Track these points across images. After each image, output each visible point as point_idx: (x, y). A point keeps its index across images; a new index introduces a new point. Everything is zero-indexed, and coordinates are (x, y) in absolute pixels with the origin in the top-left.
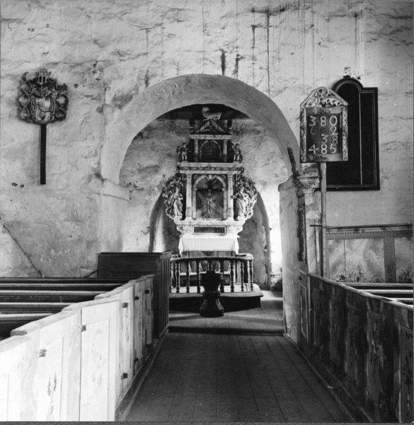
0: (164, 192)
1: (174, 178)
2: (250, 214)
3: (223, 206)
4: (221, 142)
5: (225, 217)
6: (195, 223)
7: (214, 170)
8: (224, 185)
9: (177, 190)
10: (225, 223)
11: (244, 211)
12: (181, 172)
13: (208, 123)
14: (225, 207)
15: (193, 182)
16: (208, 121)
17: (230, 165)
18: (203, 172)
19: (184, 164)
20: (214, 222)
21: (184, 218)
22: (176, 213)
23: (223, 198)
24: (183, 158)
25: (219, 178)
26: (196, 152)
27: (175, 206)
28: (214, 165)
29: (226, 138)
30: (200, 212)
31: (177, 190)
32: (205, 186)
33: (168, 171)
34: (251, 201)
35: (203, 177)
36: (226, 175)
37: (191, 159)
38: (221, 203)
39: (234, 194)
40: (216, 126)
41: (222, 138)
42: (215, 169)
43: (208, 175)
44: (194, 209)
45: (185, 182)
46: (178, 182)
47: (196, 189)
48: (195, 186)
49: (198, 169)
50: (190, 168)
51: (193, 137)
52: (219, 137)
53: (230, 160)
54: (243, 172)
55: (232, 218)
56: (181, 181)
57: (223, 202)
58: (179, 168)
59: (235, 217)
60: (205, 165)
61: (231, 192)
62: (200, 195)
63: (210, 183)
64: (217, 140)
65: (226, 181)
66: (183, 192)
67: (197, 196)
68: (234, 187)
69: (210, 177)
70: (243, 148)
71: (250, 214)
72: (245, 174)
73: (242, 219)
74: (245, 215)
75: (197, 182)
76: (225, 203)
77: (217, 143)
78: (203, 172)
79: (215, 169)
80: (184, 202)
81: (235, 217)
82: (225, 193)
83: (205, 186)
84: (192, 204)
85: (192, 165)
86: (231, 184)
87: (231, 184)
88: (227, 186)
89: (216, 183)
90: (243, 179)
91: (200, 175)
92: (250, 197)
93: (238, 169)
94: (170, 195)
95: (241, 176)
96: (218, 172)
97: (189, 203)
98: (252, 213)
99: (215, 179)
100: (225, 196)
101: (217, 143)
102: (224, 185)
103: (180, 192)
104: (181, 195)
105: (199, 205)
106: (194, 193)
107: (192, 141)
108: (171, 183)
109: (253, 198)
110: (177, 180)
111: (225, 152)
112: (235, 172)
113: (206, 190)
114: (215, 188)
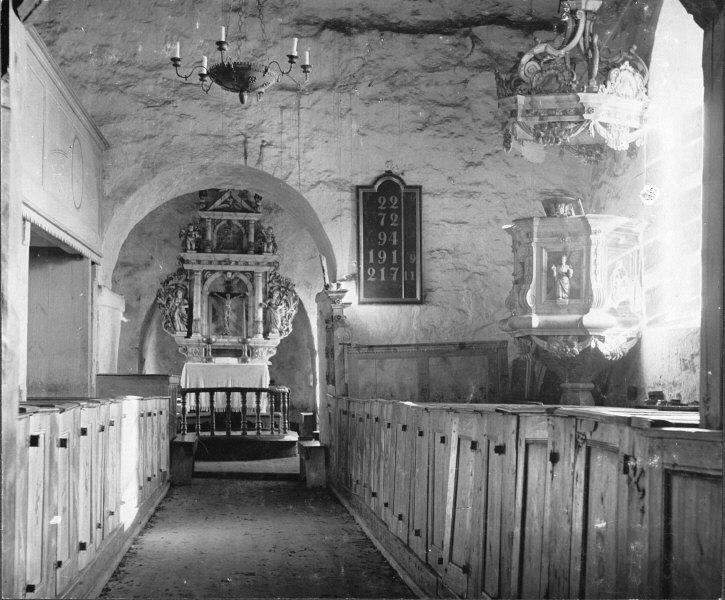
0: (159, 295)
2: (288, 330)
4: (246, 223)
7: (239, 262)
8: (250, 287)
9: (180, 294)
12: (186, 267)
13: (227, 195)
15: (204, 280)
18: (219, 268)
19: (191, 255)
21: (189, 335)
22: (178, 327)
25: (242, 277)
26: (209, 237)
27: (176, 317)
28: (234, 257)
29: (253, 217)
32: (222, 289)
33: (163, 268)
35: (218, 275)
36: (252, 273)
37: (199, 250)
38: (244, 312)
39: (264, 301)
40: (239, 200)
42: (237, 263)
43: (225, 272)
45: (191, 282)
46: (180, 282)
48: (206, 288)
49: (211, 263)
50: (199, 262)
51: (204, 215)
52: (241, 216)
53: (259, 251)
54: (277, 268)
55: (261, 336)
56: (186, 280)
58: (182, 260)
59: (266, 335)
60: (220, 257)
61: (260, 298)
62: (213, 301)
64: (239, 221)
65: (252, 280)
68: (265, 292)
70: (277, 232)
71: (288, 330)
72: (281, 272)
73: (276, 339)
74: (281, 332)
75: (209, 282)
78: (219, 268)
80: (190, 311)
81: (266, 335)
82: (251, 299)
83: (222, 289)
84: (202, 315)
85: (202, 256)
86: (260, 285)
87: (260, 285)
88: (254, 289)
90: (278, 279)
91: (213, 272)
92: (288, 305)
93: (269, 264)
94: (168, 300)
96: (242, 268)
97: (197, 313)
98: (291, 330)
100: (251, 304)
103: (185, 297)
104: (186, 301)
105: (215, 315)
109: (292, 307)
112: (267, 269)
113: (223, 295)
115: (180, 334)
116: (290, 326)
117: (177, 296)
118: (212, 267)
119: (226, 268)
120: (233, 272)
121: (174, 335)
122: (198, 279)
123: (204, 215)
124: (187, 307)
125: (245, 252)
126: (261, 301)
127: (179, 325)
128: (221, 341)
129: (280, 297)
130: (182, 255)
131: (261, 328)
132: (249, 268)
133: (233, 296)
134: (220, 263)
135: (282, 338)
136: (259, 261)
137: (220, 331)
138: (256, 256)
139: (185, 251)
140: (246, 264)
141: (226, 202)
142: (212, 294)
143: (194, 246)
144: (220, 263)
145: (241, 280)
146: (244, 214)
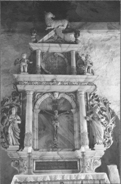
1: (10, 97)
2: (109, 141)
3: (73, 132)
5: (77, 147)
6: (37, 155)
7: (62, 85)
8: (74, 105)
9: (14, 111)
10: (79, 153)
11: (102, 137)
12: (20, 87)
13: (52, 33)
14: (77, 135)
15: (34, 103)
16: (51, 30)
17: (81, 78)
18: (47, 88)
19: (24, 77)
20: (63, 155)
21: (22, 146)
22: (11, 141)
23: (72, 121)
24: (22, 70)
25: (67, 97)
28: (61, 78)
29: (74, 48)
30: (44, 139)
31: (14, 111)
32: (50, 108)
34: (109, 125)
35: (47, 96)
36: (76, 93)
37: (32, 70)
41: (69, 50)
42: (62, 83)
43: (53, 93)
44: (36, 137)
45: (24, 102)
46: (15, 102)
47: (39, 111)
48: (37, 107)
49: (40, 83)
50: (30, 83)
52: (65, 48)
53: (80, 72)
54: (95, 90)
55: (88, 147)
56: (20, 101)
57: (73, 126)
58: (16, 83)
59: (92, 146)
60: (49, 77)
61: (83, 111)
63: (55, 103)
64: (62, 53)
66: (22, 113)
67: (39, 119)
69: (57, 96)
70: (92, 60)
71: (109, 141)
72: (97, 93)
75: (39, 102)
76: (76, 128)
77: (62, 56)
78: (47, 88)
79: (62, 83)
80: (22, 126)
81: (92, 146)
82: (75, 115)
84: (33, 131)
85: (34, 77)
86: (83, 103)
87: (83, 103)
88: (78, 107)
89: (64, 103)
90: (95, 96)
91: (43, 94)
93: (90, 84)
95: (94, 94)
96: (67, 89)
97: (29, 128)
98: (112, 142)
99: (62, 98)
100: (76, 119)
101: (62, 56)
102: (74, 105)
103: (18, 113)
104: (19, 118)
106: (36, 116)
107: (34, 53)
108: (6, 103)
109: (111, 123)
110: (14, 100)
111: (74, 64)
114: (62, 109)
115: (13, 146)
116: (111, 138)
117: (11, 113)
118: (40, 88)
119: (54, 88)
120: (60, 93)
121: (6, 150)
122: (30, 98)
123: (34, 46)
124: (20, 122)
125: (71, 73)
126: (85, 115)
127: (11, 138)
128: (52, 155)
129: (100, 113)
130: (16, 75)
131: (87, 141)
132: (74, 88)
133: (60, 112)
134: (48, 83)
135: (105, 149)
136: (82, 80)
137: (52, 146)
138: (79, 76)
139: (19, 72)
140: (70, 84)
141: (52, 38)
142: (42, 112)
143: (26, 70)
144: (48, 83)
145: (66, 100)
146: (68, 45)
